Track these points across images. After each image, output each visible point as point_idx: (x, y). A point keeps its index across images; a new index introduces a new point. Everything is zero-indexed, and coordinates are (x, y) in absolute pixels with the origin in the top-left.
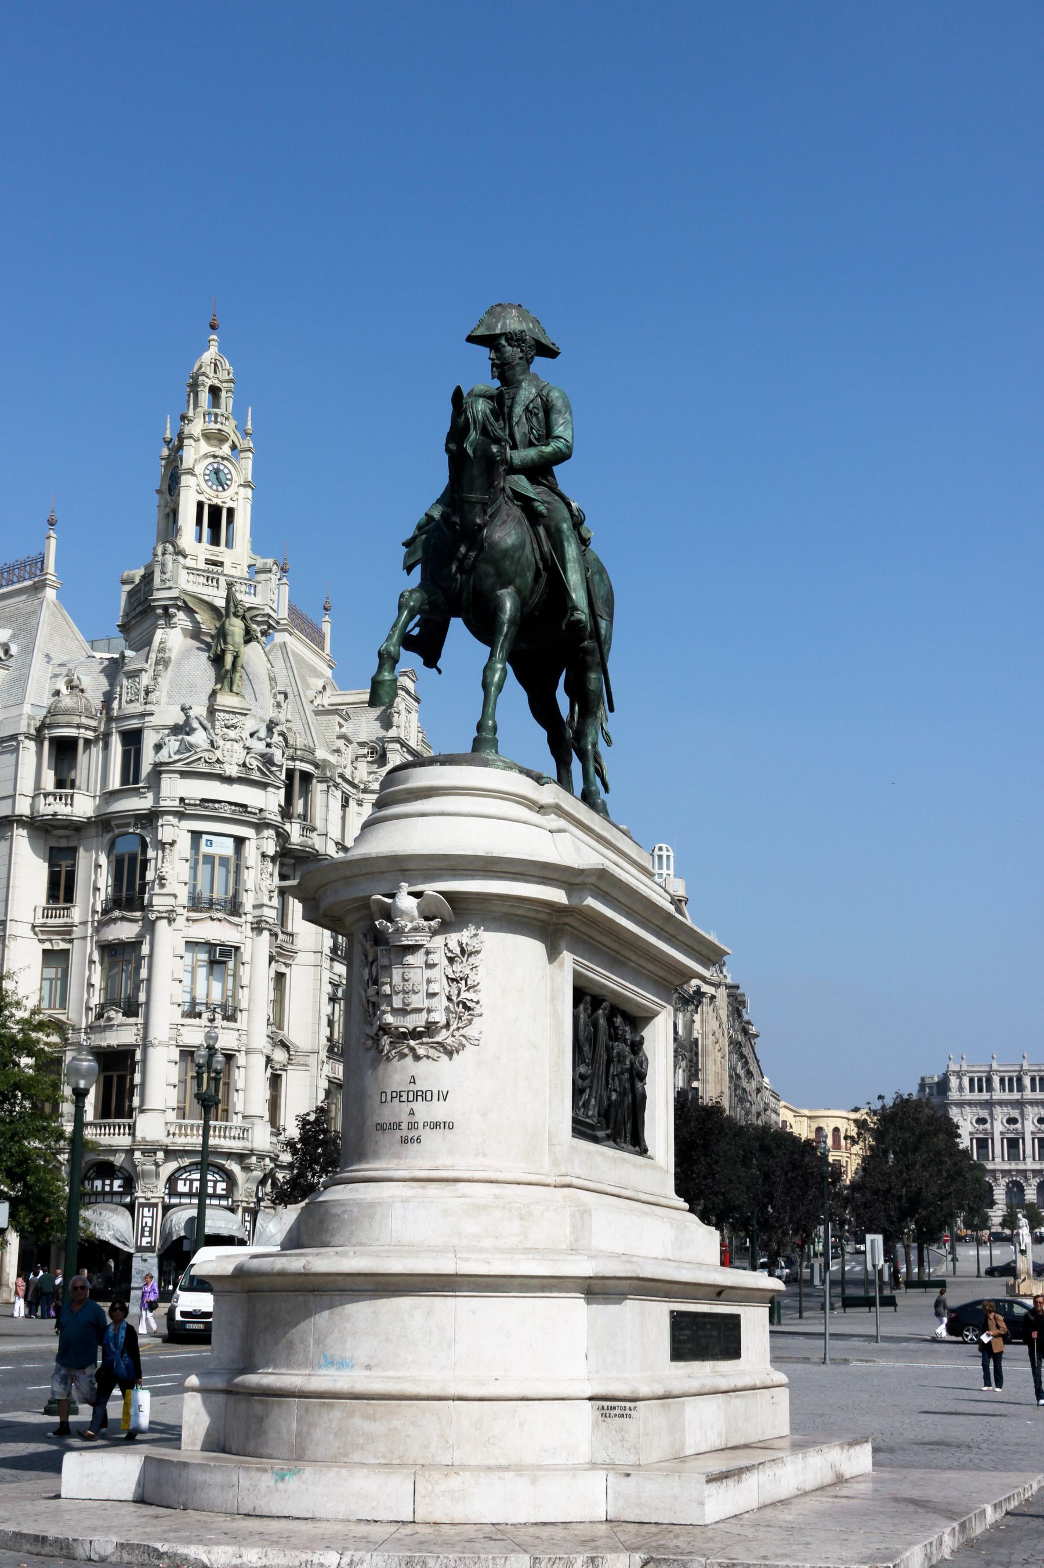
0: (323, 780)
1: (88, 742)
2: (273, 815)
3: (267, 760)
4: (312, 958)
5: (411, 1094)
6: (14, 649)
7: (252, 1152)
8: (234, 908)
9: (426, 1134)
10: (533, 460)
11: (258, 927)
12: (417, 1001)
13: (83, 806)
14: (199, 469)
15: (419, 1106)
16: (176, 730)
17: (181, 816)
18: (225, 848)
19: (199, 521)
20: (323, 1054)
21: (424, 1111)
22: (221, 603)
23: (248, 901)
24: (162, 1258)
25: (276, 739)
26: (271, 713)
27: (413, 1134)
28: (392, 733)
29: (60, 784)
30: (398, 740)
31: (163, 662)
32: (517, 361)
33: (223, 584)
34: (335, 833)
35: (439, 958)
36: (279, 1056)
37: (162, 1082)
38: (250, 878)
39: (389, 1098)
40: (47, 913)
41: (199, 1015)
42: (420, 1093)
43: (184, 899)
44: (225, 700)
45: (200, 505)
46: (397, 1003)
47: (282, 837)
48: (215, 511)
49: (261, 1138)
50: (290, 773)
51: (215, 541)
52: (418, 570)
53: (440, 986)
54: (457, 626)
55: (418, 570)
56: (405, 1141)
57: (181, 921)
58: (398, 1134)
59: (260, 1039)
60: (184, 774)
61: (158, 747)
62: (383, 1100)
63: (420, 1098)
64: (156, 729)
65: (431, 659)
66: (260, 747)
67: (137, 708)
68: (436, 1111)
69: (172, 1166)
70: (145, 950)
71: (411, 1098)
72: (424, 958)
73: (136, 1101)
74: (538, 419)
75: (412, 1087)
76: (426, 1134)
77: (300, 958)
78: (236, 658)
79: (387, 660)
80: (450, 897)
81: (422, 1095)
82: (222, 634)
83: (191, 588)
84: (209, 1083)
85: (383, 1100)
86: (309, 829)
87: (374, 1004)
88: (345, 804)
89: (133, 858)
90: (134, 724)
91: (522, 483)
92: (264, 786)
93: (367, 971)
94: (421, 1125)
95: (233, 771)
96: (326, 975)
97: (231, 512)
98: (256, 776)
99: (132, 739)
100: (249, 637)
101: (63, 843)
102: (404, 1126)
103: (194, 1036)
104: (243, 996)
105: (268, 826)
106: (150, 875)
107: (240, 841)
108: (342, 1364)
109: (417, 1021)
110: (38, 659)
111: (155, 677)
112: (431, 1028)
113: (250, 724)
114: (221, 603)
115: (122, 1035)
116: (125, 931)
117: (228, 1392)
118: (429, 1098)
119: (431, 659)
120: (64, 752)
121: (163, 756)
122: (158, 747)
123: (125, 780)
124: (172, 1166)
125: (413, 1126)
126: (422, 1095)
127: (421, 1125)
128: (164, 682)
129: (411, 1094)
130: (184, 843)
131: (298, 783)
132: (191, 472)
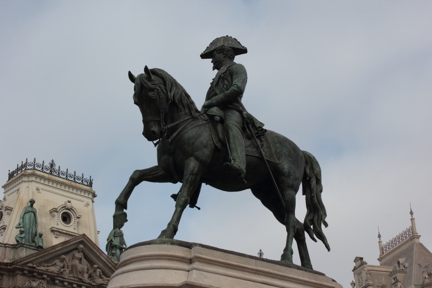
10: (222, 99)
32: (222, 59)
74: (227, 80)
91: (215, 110)
110: (415, 267)
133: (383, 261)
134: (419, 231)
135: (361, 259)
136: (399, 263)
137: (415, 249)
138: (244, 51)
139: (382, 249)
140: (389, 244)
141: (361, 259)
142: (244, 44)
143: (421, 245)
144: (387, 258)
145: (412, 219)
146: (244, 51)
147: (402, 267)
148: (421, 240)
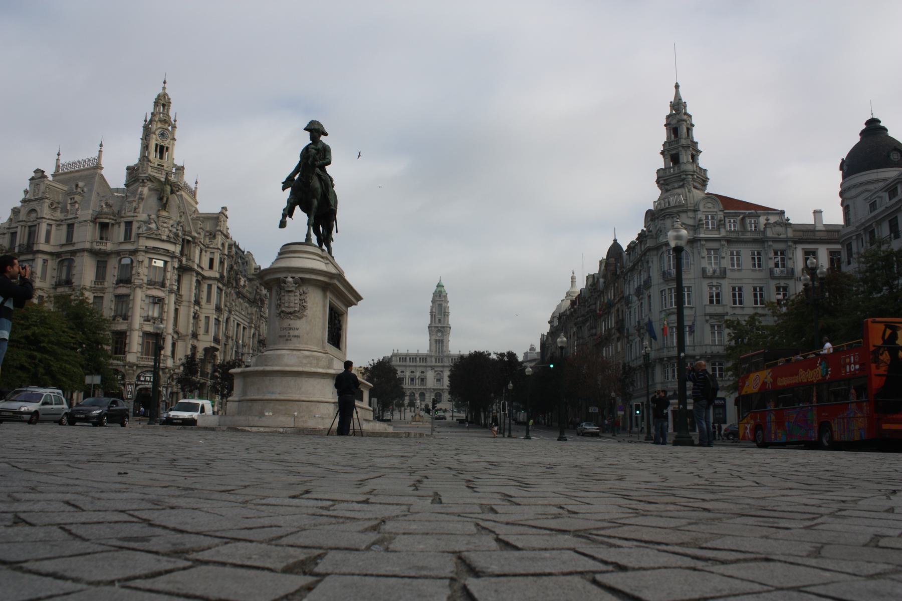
0: (194, 243)
1: (113, 225)
2: (178, 254)
3: (177, 235)
4: (187, 304)
6: (85, 190)
7: (167, 368)
8: (163, 285)
9: (293, 339)
11: (171, 291)
12: (292, 305)
13: (109, 247)
14: (157, 132)
15: (291, 331)
16: (145, 222)
17: (146, 252)
18: (160, 264)
19: (156, 151)
20: (190, 336)
21: (292, 333)
22: (163, 180)
23: (168, 283)
24: (135, 401)
25: (180, 228)
26: (178, 219)
28: (218, 228)
29: (102, 238)
30: (220, 231)
31: (141, 199)
33: (164, 173)
34: (197, 261)
35: (298, 294)
36: (176, 336)
37: (135, 343)
38: (169, 275)
40: (96, 283)
41: (149, 321)
43: (145, 281)
44: (165, 214)
45: (157, 145)
46: (286, 305)
47: (180, 261)
48: (162, 148)
49: (170, 363)
50: (183, 240)
51: (161, 158)
52: (289, 190)
54: (297, 208)
55: (289, 190)
57: (144, 289)
59: (170, 330)
60: (147, 238)
61: (139, 228)
64: (138, 222)
65: (290, 216)
66: (175, 230)
67: (131, 214)
68: (296, 333)
69: (139, 371)
70: (131, 298)
73: (127, 349)
76: (293, 339)
77: (184, 303)
78: (167, 199)
79: (284, 216)
80: (301, 278)
81: (292, 329)
82: (163, 191)
83: (152, 174)
84: (154, 341)
86: (188, 259)
88: (201, 252)
89: (128, 265)
90: (130, 219)
92: (175, 244)
95: (164, 238)
96: (192, 310)
97: (167, 148)
98: (172, 240)
99: (129, 224)
100: (172, 192)
101: (102, 259)
103: (149, 328)
104: (165, 315)
105: (176, 257)
106: (134, 272)
107: (166, 262)
108: (273, 393)
109: (292, 310)
110: (94, 194)
111: (139, 203)
112: (295, 312)
113: (171, 222)
114: (163, 180)
115: (121, 326)
116: (123, 291)
117: (239, 401)
119: (290, 216)
120: (104, 226)
121: (140, 231)
122: (139, 228)
123: (125, 239)
124: (139, 371)
126: (292, 329)
128: (141, 206)
130: (146, 262)
131: (186, 243)
132: (154, 133)
133: (58, 178)
134: (103, 163)
135: (43, 172)
136: (77, 186)
137: (97, 178)
138: (326, 134)
139: (58, 166)
140: (67, 165)
141: (43, 172)
142: (327, 130)
143: (102, 176)
144: (63, 177)
145: (100, 151)
146: (326, 134)
147: (79, 190)
148: (103, 172)
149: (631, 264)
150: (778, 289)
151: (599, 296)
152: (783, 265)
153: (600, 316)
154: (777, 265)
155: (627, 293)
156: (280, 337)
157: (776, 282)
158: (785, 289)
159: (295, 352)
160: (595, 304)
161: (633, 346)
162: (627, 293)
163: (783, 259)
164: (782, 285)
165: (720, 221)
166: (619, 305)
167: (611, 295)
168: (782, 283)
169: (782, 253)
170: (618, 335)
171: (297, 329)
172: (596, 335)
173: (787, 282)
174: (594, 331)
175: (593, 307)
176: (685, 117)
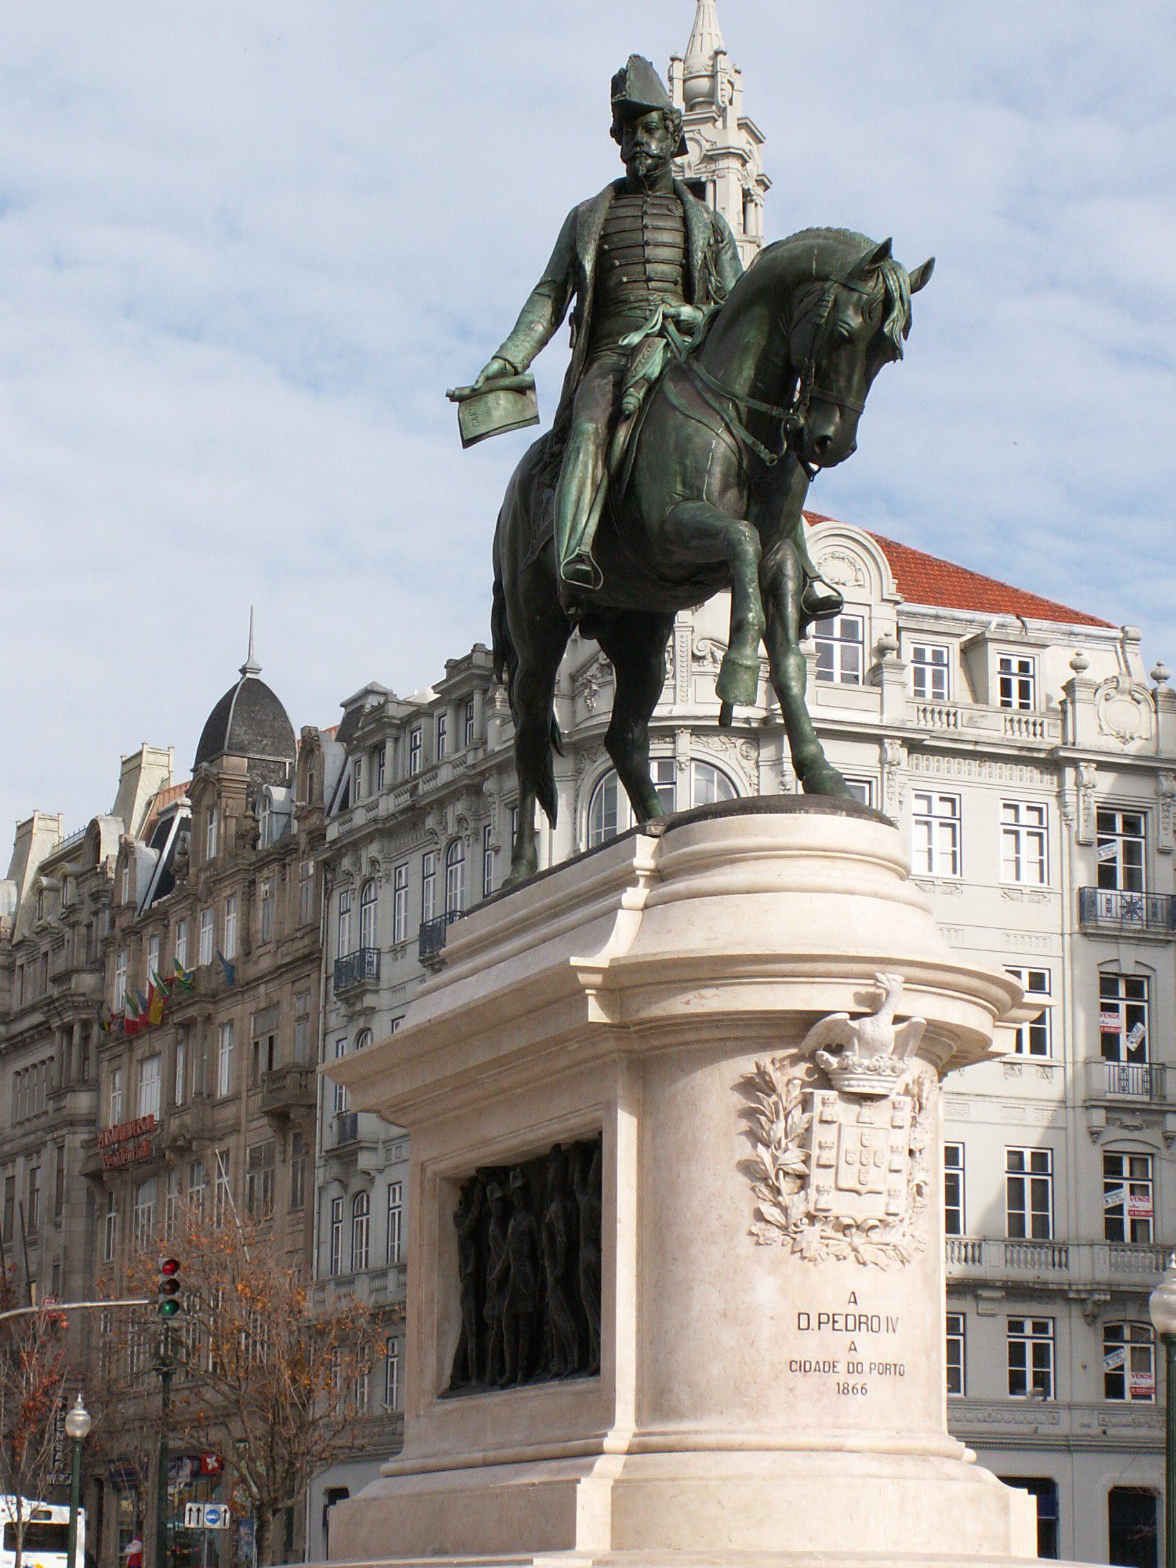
5: (851, 1319)
12: (876, 1178)
27: (853, 1380)
35: (904, 1116)
39: (814, 1323)
42: (863, 1319)
53: (902, 1161)
56: (844, 1390)
58: (833, 1379)
62: (804, 1324)
63: (863, 1326)
71: (851, 1326)
72: (888, 1118)
75: (852, 1309)
76: (872, 1380)
81: (864, 1322)
85: (804, 1324)
87: (786, 1174)
93: (782, 1124)
94: (866, 1368)
102: (841, 1367)
118: (875, 1328)
125: (854, 1368)
126: (864, 1322)
127: (866, 1368)
129: (851, 1319)
149: (388, 805)
150: (1108, 985)
151: (134, 932)
152: (1133, 881)
153: (132, 1031)
154: (1106, 876)
155: (342, 940)
156: (802, 1367)
157: (1106, 951)
158: (1135, 988)
159: (909, 1466)
160: (99, 966)
161: (378, 1195)
162: (342, 940)
163: (1131, 852)
164: (1128, 968)
165: (882, 651)
166: (282, 991)
167: (212, 939)
168: (1128, 960)
169: (1131, 826)
170: (260, 1131)
171: (891, 1325)
172: (92, 1121)
173: (1149, 955)
174: (81, 1102)
175: (86, 982)
176: (739, 140)
